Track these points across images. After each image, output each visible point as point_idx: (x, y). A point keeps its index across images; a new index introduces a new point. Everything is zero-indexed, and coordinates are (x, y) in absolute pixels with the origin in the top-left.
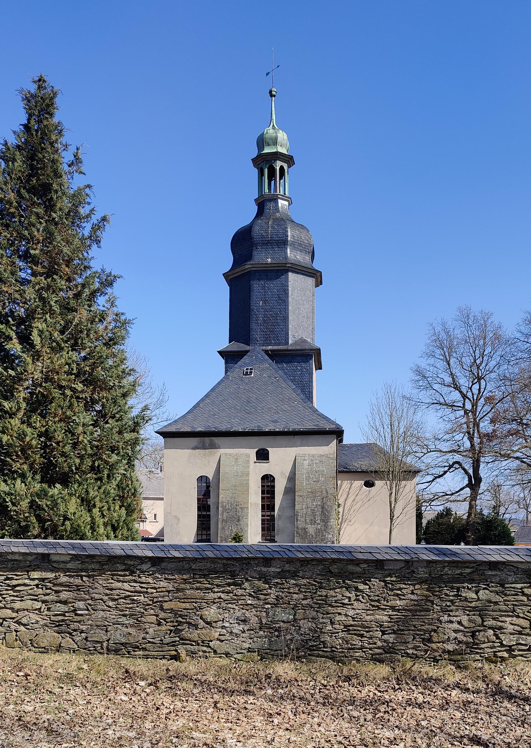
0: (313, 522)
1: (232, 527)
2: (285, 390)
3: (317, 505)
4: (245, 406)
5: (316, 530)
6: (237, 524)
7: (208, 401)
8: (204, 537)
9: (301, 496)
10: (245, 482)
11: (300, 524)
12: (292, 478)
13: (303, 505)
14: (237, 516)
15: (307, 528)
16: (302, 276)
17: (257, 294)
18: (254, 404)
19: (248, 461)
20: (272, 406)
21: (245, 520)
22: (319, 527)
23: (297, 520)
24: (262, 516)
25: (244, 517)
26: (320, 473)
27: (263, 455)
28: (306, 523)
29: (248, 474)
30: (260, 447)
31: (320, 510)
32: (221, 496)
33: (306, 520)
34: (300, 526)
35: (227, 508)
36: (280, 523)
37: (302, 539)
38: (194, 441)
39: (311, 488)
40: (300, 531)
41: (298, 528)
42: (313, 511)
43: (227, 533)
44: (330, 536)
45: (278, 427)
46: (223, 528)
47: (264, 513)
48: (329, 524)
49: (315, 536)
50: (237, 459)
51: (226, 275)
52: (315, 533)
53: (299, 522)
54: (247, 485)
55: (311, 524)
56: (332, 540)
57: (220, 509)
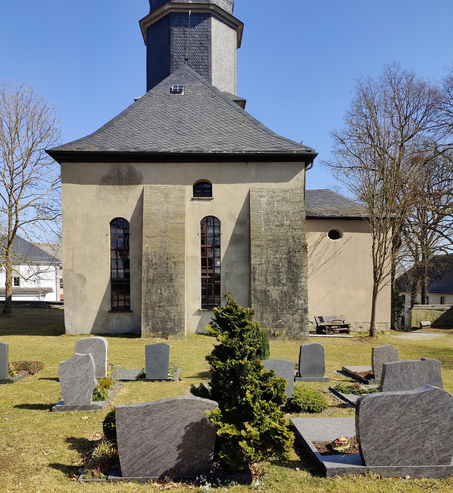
0: (277, 282)
1: (161, 290)
2: (228, 110)
3: (281, 259)
4: (175, 126)
5: (282, 292)
6: (168, 286)
7: (124, 119)
8: (121, 304)
9: (258, 246)
10: (179, 226)
11: (258, 285)
12: (245, 221)
13: (261, 258)
14: (168, 275)
15: (269, 291)
16: (224, 25)
17: (177, 39)
18: (188, 124)
19: (183, 197)
20: (212, 127)
21: (180, 279)
22: (285, 289)
23: (254, 279)
24: (203, 274)
25: (179, 276)
26: (284, 214)
27: (203, 190)
28: (267, 284)
29: (183, 215)
30: (199, 178)
31: (286, 265)
32: (145, 246)
33: (266, 279)
34: (259, 288)
35: (154, 262)
36: (228, 284)
37: (262, 305)
38: (104, 168)
39: (273, 235)
40: (258, 295)
41: (255, 291)
42: (276, 267)
43: (154, 297)
44: (301, 302)
45: (226, 148)
46: (149, 292)
47: (205, 271)
48: (299, 284)
49: (280, 302)
50: (167, 195)
51: (142, 23)
52: (280, 297)
53: (257, 283)
54: (182, 230)
55: (274, 285)
56: (304, 307)
57: (144, 264)
